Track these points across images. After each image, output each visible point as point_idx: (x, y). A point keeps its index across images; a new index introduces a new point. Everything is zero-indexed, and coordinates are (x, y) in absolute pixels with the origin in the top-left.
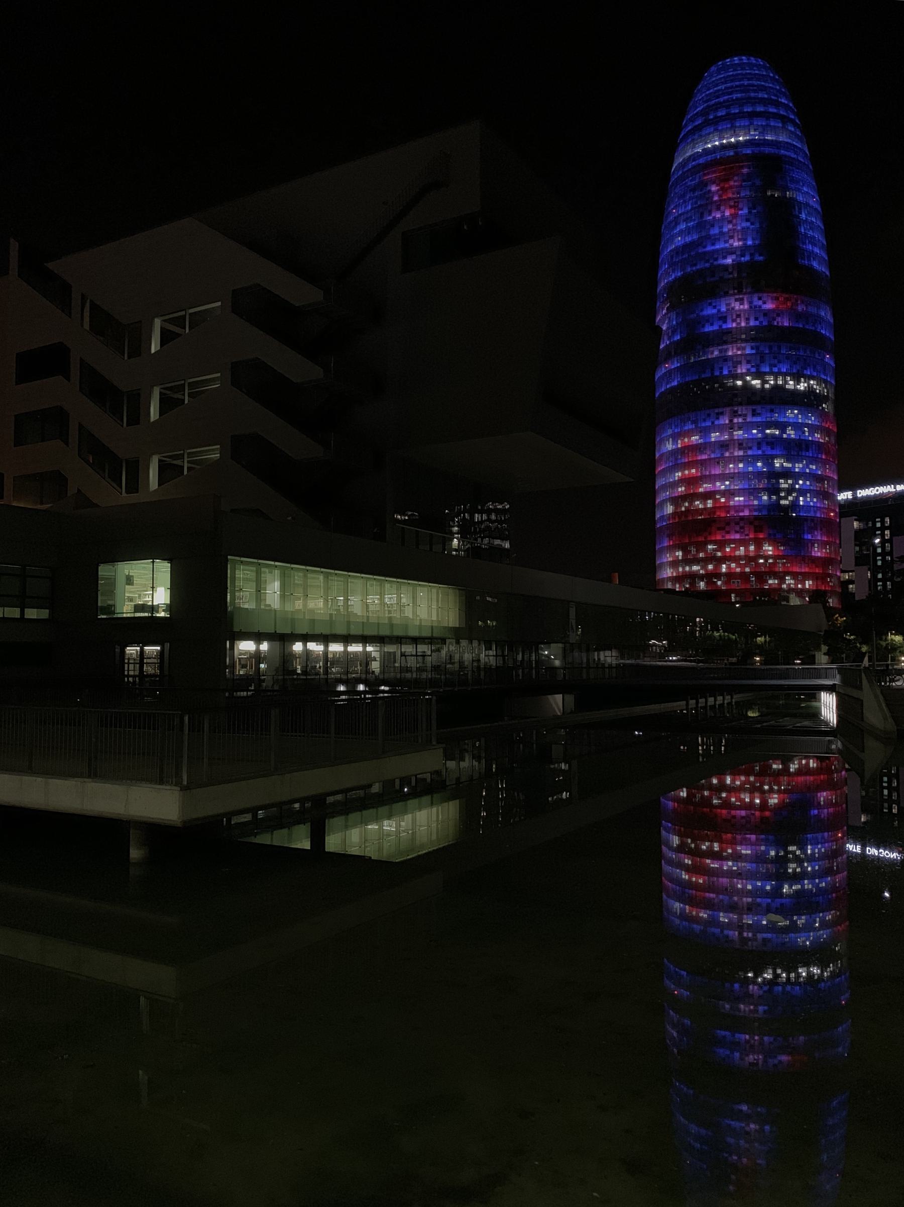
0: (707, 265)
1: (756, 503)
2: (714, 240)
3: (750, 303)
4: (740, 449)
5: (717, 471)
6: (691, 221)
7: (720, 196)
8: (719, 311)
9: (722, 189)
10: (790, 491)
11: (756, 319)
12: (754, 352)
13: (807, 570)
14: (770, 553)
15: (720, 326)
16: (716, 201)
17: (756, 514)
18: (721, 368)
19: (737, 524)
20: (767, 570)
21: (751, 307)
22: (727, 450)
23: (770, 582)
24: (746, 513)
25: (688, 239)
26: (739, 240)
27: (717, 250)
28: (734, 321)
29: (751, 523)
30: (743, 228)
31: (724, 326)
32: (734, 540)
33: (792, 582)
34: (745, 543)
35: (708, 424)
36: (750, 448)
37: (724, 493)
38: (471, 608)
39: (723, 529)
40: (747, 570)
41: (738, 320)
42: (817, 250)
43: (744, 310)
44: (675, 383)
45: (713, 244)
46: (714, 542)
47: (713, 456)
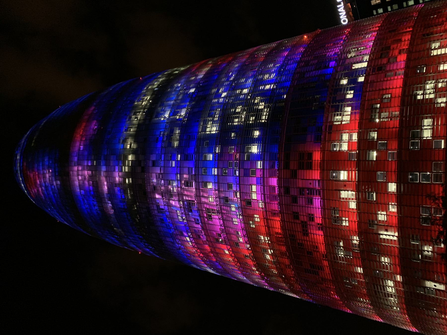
1: (259, 165)
5: (217, 220)
10: (251, 109)
13: (403, 58)
14: (355, 137)
19: (295, 200)
20: (394, 144)
23: (427, 134)
24: (274, 182)
29: (294, 175)
32: (323, 208)
33: (430, 86)
34: (331, 189)
37: (247, 217)
39: (304, 225)
40: (392, 187)
46: (331, 246)
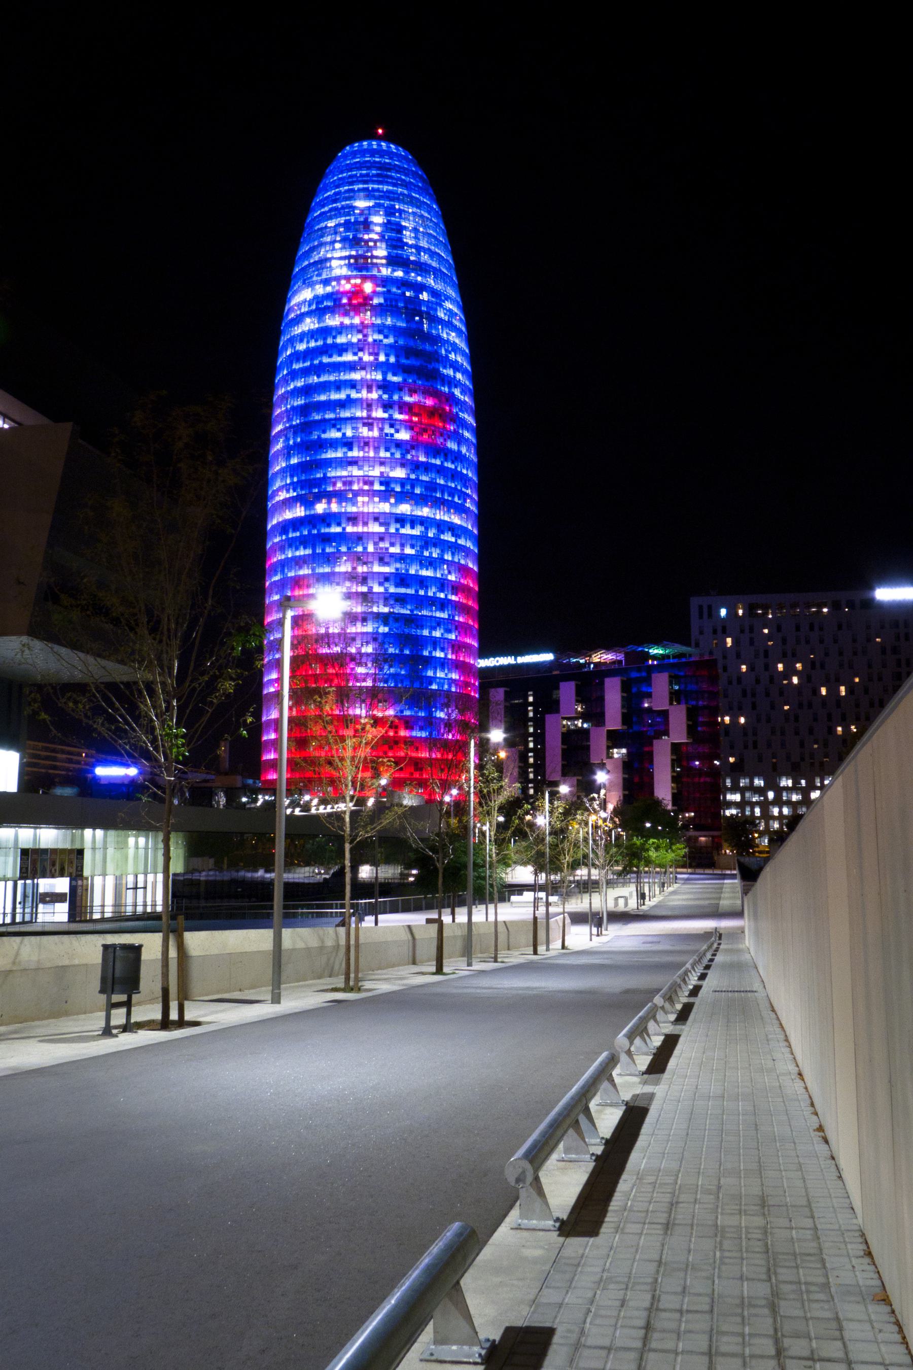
2: (342, 349)
3: (381, 430)
8: (344, 434)
11: (387, 450)
12: (383, 488)
21: (381, 435)
25: (313, 344)
26: (370, 354)
31: (350, 454)
41: (366, 449)
42: (459, 376)
43: (374, 438)
45: (340, 355)
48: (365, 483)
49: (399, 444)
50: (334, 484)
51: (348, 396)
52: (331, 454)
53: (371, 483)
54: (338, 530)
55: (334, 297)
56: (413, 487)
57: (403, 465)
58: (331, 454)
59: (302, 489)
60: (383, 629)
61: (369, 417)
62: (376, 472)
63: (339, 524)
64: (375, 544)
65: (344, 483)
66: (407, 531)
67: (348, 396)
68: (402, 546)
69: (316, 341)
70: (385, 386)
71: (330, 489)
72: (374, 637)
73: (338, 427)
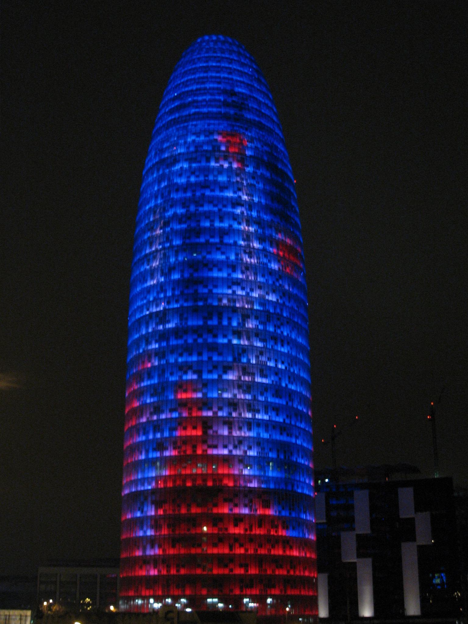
0: (216, 209)
2: (223, 188)
4: (249, 411)
6: (195, 162)
7: (227, 148)
8: (228, 258)
9: (228, 142)
11: (263, 276)
15: (229, 275)
16: (223, 152)
17: (263, 486)
18: (230, 320)
19: (246, 496)
22: (235, 410)
27: (227, 198)
28: (243, 273)
30: (251, 184)
31: (234, 275)
35: (215, 376)
36: (258, 412)
38: (219, 599)
44: (170, 326)
47: (220, 414)
48: (248, 303)
49: (271, 272)
50: (220, 300)
51: (231, 226)
52: (215, 274)
53: (252, 303)
54: (225, 341)
55: (214, 144)
56: (282, 310)
57: (274, 291)
58: (215, 274)
59: (186, 301)
60: (265, 435)
61: (249, 246)
62: (255, 294)
63: (225, 336)
64: (257, 357)
65: (229, 301)
66: (280, 348)
67: (231, 226)
68: (276, 361)
69: (197, 176)
70: (258, 222)
71: (215, 303)
72: (258, 442)
73: (223, 250)
